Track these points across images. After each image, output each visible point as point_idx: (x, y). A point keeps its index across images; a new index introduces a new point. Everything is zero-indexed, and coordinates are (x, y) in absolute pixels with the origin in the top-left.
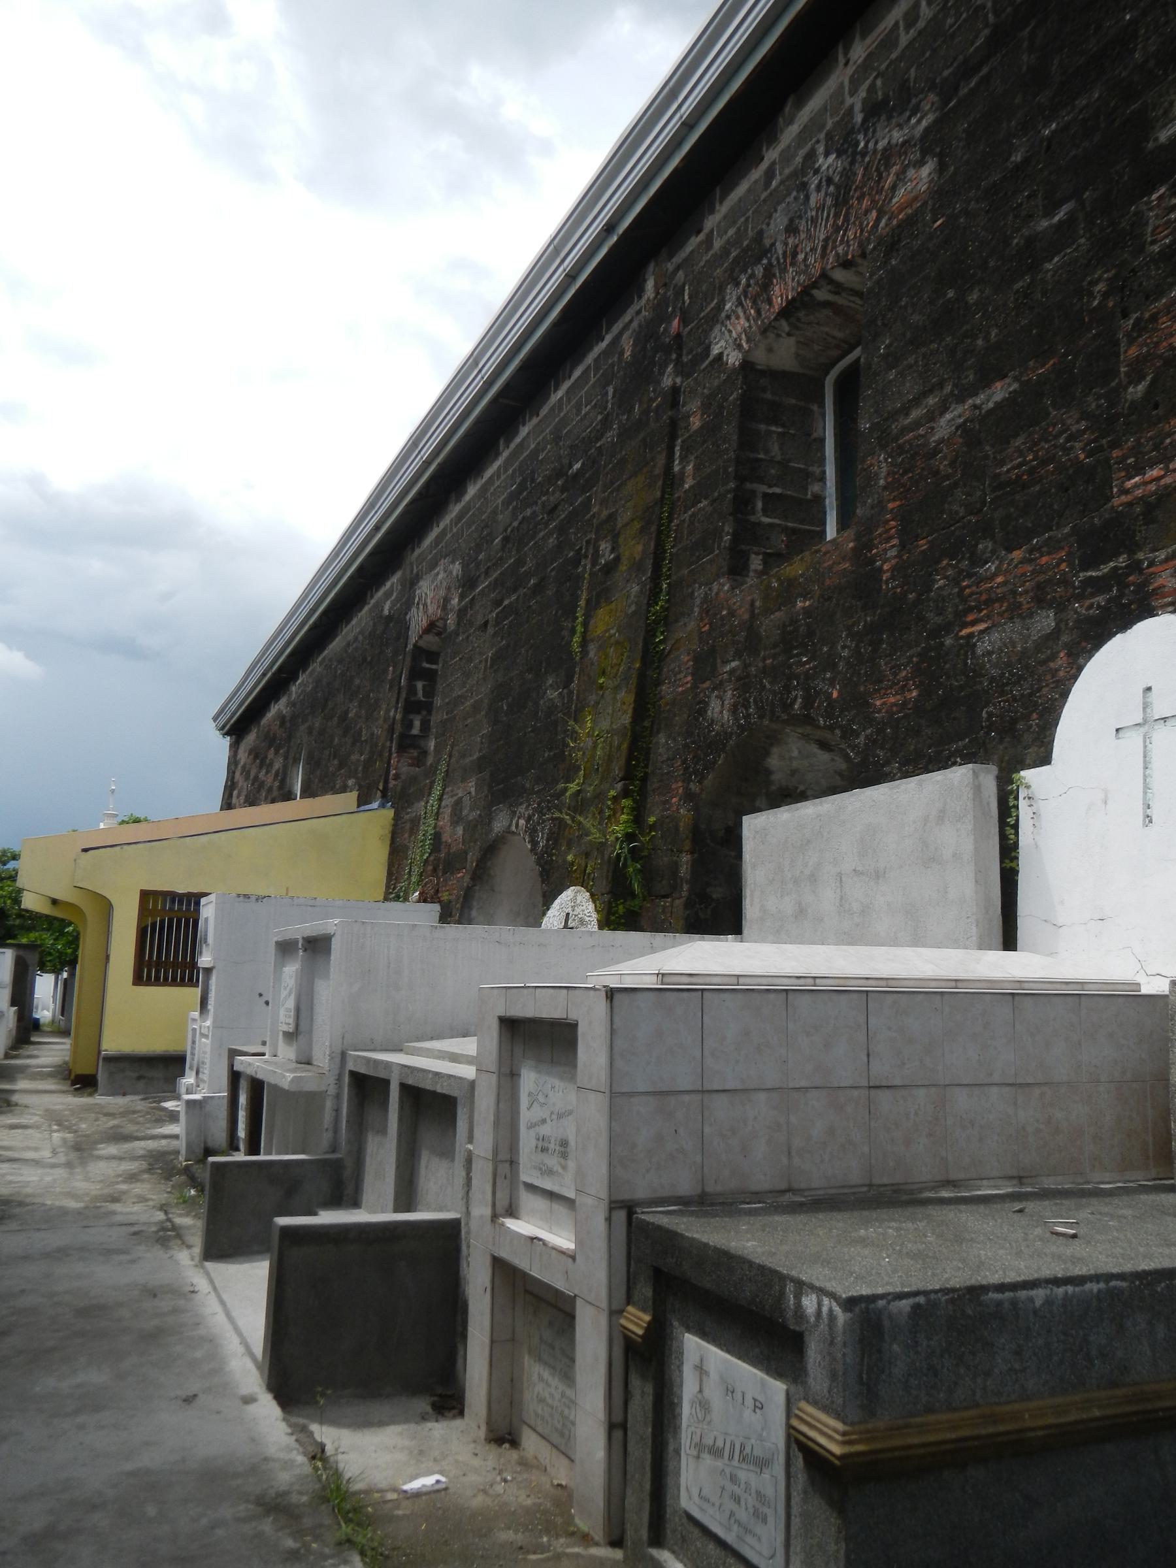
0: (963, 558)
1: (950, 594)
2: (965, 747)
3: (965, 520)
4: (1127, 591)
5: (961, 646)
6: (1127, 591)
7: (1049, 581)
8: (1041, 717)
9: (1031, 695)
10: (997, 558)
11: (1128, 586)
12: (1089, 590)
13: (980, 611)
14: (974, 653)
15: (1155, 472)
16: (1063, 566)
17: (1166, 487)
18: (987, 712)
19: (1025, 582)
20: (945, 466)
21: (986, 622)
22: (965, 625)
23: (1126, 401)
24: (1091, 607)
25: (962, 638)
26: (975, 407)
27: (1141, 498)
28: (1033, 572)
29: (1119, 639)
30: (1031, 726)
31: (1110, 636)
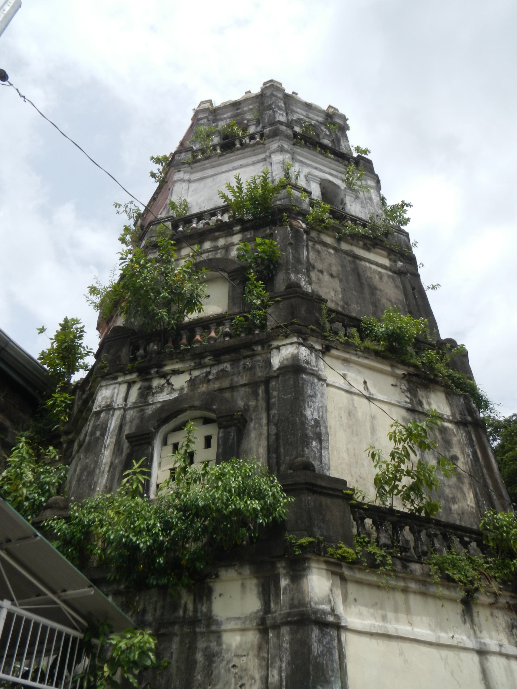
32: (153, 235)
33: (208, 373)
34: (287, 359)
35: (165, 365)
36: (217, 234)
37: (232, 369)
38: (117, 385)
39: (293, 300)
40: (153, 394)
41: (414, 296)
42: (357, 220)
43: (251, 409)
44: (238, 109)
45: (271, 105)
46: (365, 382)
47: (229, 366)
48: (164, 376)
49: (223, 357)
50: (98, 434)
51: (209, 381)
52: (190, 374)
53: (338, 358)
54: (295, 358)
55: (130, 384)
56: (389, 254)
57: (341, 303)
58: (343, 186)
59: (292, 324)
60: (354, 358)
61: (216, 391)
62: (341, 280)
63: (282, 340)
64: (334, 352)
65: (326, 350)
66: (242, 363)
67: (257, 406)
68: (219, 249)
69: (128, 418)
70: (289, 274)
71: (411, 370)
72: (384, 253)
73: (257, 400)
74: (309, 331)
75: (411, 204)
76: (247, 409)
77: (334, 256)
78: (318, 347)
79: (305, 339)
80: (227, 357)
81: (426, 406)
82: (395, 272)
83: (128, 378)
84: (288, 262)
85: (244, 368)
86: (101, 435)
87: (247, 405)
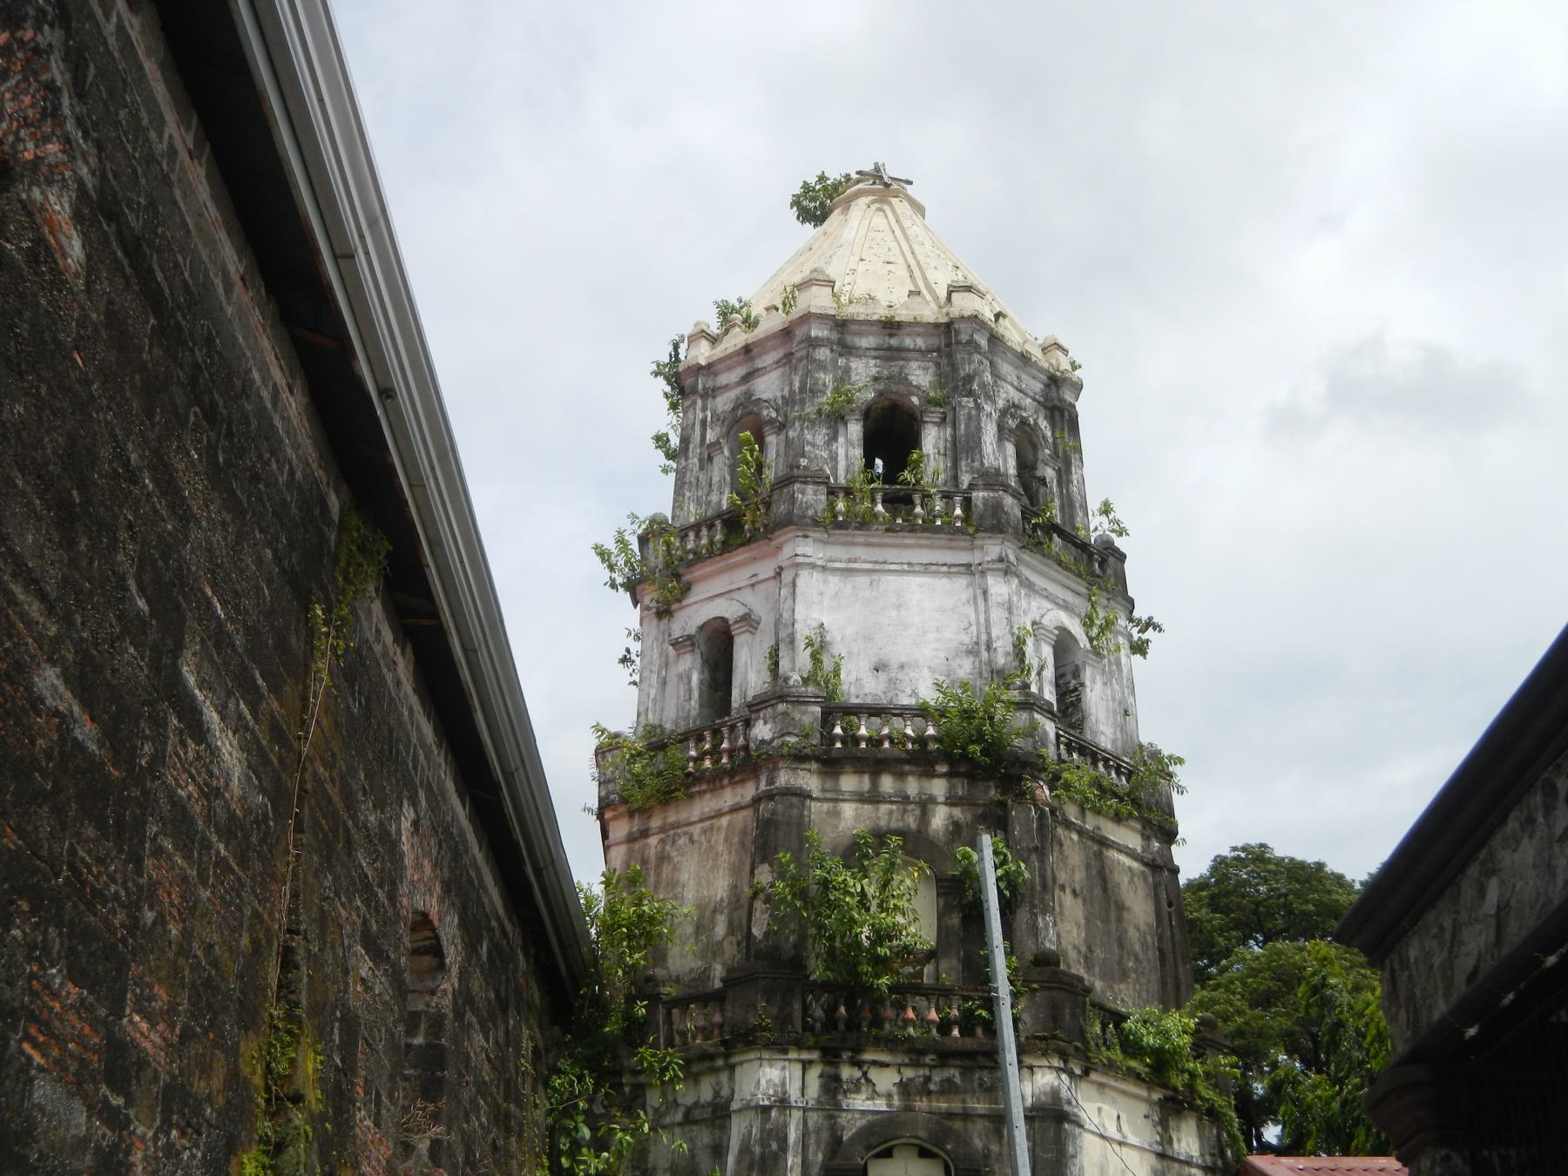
32: (791, 730)
33: (928, 1079)
34: (1045, 1093)
35: (864, 1051)
36: (907, 768)
37: (963, 1081)
38: (787, 1063)
39: (1055, 994)
40: (845, 1092)
41: (1171, 921)
42: (1109, 759)
43: (994, 1157)
44: (891, 335)
45: (969, 379)
46: (1119, 1117)
47: (957, 1075)
48: (858, 1064)
49: (952, 1062)
50: (774, 1146)
51: (929, 1093)
52: (899, 1072)
53: (1093, 1082)
54: (1055, 1093)
55: (806, 1065)
56: (1144, 827)
57: (1083, 949)
58: (1084, 642)
59: (1054, 1037)
60: (1112, 1083)
61: (940, 1114)
62: (1084, 901)
63: (1037, 1057)
64: (1094, 1076)
65: (1086, 1072)
66: (977, 1076)
67: (1000, 1154)
68: (911, 803)
69: (811, 1124)
70: (1036, 915)
71: (1170, 1093)
72: (1139, 826)
73: (1001, 1144)
74: (1072, 1051)
75: (1163, 627)
76: (987, 1156)
77: (1077, 848)
78: (1078, 1071)
79: (1065, 1062)
80: (959, 1063)
81: (1176, 1145)
82: (1146, 864)
83: (805, 1056)
84: (1033, 889)
85: (981, 1085)
86: (779, 1147)
87: (985, 1147)
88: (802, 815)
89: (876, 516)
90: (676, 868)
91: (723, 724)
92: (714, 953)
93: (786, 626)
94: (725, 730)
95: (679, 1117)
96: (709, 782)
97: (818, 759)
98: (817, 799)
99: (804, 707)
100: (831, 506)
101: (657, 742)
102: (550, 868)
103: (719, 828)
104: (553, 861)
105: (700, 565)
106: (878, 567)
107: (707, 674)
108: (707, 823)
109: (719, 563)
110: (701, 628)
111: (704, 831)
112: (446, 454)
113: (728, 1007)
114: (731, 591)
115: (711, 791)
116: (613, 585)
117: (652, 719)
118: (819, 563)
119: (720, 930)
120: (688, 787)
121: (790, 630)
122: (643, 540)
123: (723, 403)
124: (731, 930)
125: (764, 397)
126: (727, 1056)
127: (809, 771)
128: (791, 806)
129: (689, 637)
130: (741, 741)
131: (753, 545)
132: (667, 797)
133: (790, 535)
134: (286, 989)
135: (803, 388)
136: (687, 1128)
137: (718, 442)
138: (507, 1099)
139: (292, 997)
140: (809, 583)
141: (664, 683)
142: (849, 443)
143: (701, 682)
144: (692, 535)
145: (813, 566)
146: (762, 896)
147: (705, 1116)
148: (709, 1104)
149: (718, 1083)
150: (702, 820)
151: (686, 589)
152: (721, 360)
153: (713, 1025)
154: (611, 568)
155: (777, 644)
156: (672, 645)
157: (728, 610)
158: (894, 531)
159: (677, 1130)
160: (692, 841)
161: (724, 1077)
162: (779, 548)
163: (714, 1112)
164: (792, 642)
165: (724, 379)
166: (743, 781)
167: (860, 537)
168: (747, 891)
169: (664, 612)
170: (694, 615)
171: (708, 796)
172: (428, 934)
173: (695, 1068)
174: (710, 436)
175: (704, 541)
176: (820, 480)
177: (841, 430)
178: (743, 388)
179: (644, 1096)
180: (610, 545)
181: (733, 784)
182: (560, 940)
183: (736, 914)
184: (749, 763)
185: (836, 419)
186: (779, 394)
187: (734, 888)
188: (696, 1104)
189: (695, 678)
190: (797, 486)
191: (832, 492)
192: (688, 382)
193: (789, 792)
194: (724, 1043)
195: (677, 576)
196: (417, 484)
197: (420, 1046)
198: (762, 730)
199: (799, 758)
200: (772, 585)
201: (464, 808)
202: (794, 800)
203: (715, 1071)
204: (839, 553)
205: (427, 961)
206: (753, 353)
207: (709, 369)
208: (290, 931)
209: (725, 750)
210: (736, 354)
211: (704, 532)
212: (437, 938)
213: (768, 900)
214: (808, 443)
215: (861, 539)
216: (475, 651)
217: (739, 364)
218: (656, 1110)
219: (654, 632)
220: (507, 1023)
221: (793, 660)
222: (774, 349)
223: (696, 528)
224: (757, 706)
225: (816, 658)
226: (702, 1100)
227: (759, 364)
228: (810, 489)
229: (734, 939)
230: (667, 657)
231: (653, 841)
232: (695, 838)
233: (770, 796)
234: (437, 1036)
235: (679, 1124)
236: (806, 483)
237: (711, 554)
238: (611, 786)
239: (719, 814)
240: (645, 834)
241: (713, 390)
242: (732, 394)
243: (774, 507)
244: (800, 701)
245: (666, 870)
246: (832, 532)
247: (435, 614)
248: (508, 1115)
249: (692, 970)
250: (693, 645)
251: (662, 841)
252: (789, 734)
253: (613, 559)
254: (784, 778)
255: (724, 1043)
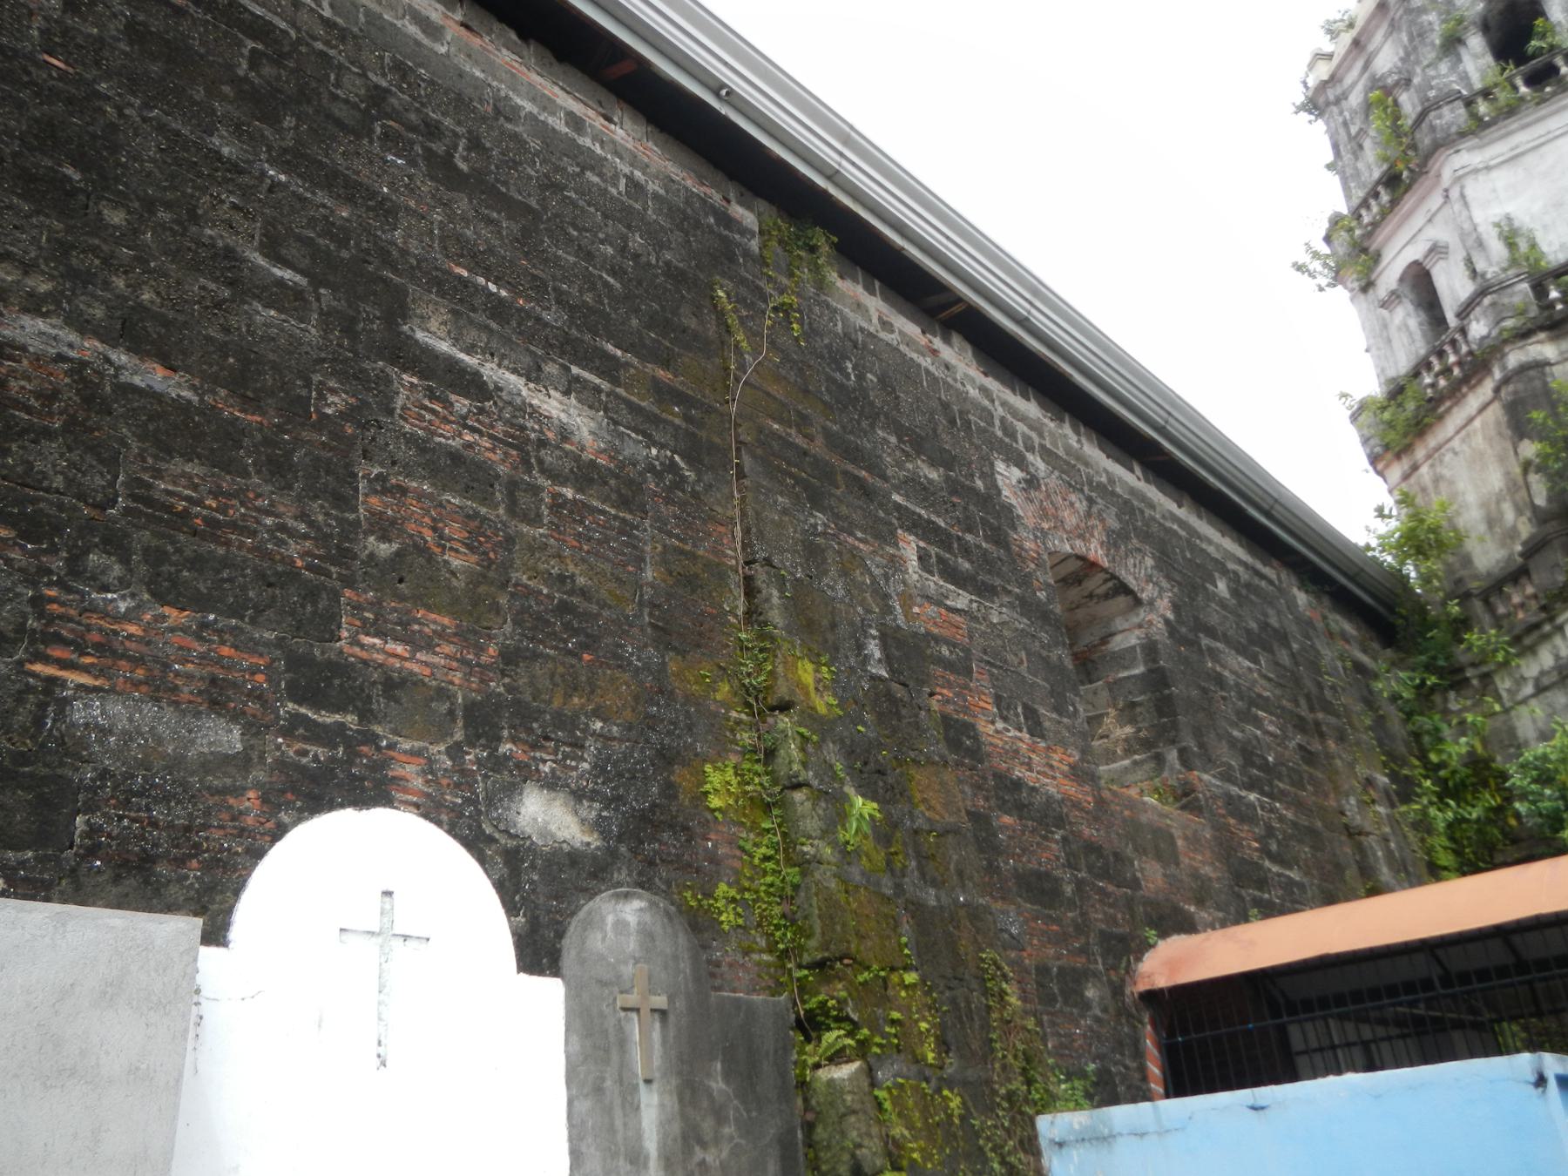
0: (53, 550)
1: (9, 590)
2: (22, 864)
3: (66, 500)
4: (358, 761)
5: (29, 689)
6: (358, 761)
7: (234, 685)
8: (207, 867)
9: (188, 829)
10: (133, 596)
11: (360, 755)
12: (301, 731)
13: (83, 654)
14: (61, 714)
15: (399, 649)
16: (260, 678)
17: (412, 673)
18: (88, 822)
19: (188, 661)
20: (23, 388)
21: (96, 678)
22: (47, 660)
23: (365, 547)
24: (305, 753)
25: (34, 675)
26: (108, 360)
27: (381, 665)
28: (202, 657)
29: (349, 813)
30: (186, 877)
31: (331, 806)
32: (1505, 315)
88: (1545, 384)
89: (1522, 99)
90: (1451, 483)
91: (1443, 343)
92: (1512, 538)
93: (1469, 234)
94: (1447, 348)
95: (1529, 689)
96: (1450, 398)
97: (1542, 328)
98: (1557, 363)
99: (1509, 290)
100: (1474, 116)
101: (1397, 391)
102: (1277, 507)
103: (1475, 431)
104: (1276, 501)
105: (1379, 230)
106: (1542, 140)
107: (1423, 316)
108: (1463, 433)
109: (1394, 220)
110: (1402, 280)
111: (1463, 441)
112: (849, 136)
113: (1535, 577)
114: (1415, 236)
115: (1456, 404)
116: (1321, 289)
117: (1392, 373)
118: (1481, 166)
119: (1509, 515)
120: (1435, 409)
121: (1474, 236)
122: (1328, 239)
123: (1355, 99)
124: (1519, 511)
125: (1385, 70)
126: (1551, 619)
127: (1538, 342)
128: (1531, 379)
129: (1393, 293)
130: (1464, 349)
131: (1415, 187)
132: (1420, 427)
133: (1442, 158)
134: (753, 615)
135: (1411, 39)
136: (1541, 697)
137: (1361, 129)
138: (1312, 709)
139: (761, 618)
140: (1473, 189)
141: (1389, 341)
142: (1475, 56)
143: (1421, 324)
144: (1363, 212)
145: (1476, 171)
146: (1532, 468)
147: (1554, 679)
148: (1554, 668)
149: (1555, 647)
150: (1458, 432)
151: (1377, 258)
152: (1339, 66)
153: (1528, 598)
154: (1312, 275)
155: (1468, 255)
156: (1382, 306)
157: (1415, 253)
158: (1547, 100)
159: (1533, 702)
160: (1456, 453)
161: (1558, 640)
162: (1439, 176)
163: (1560, 673)
164: (1480, 244)
165: (1348, 80)
166: (1480, 382)
167: (1513, 123)
168: (1518, 470)
169: (1367, 287)
170: (1390, 274)
171: (1455, 410)
172: (1103, 576)
173: (1527, 641)
174: (1354, 130)
175: (1375, 209)
176: (1451, 97)
177: (1462, 51)
178: (1366, 75)
179: (1493, 683)
180: (1304, 258)
181: (1472, 388)
182: (1345, 574)
183: (1517, 497)
184: (1476, 366)
185: (1452, 43)
186: (1396, 59)
187: (1507, 474)
188: (1543, 673)
189: (1413, 323)
190: (1432, 114)
191: (1469, 103)
192: (1321, 100)
193: (1523, 368)
194: (1544, 608)
195: (1365, 250)
196: (833, 175)
197: (1143, 674)
198: (1479, 328)
199: (1523, 335)
200: (1446, 211)
201: (1132, 471)
202: (1532, 373)
203: (1546, 637)
204: (1498, 150)
205: (1122, 601)
206: (1363, 39)
207: (1333, 79)
208: (747, 563)
209: (1454, 364)
210: (1349, 52)
211: (1373, 202)
212: (1113, 577)
213: (1539, 470)
214: (1434, 78)
215: (1515, 126)
216: (1027, 319)
217: (1355, 60)
218: (1509, 691)
219: (1364, 305)
220: (1289, 647)
221: (1488, 259)
222: (1377, 27)
223: (1365, 204)
224: (1465, 312)
225: (1511, 245)
226: (1546, 668)
227: (1371, 48)
228: (1446, 110)
229: (1524, 519)
230: (1384, 319)
231: (1424, 470)
232: (1457, 450)
233: (1506, 381)
234: (1155, 661)
235: (1534, 696)
236: (1439, 107)
237: (1385, 214)
238: (1372, 442)
239: (1471, 420)
240: (1415, 468)
241: (1343, 93)
242: (1360, 87)
243: (1420, 146)
244: (1503, 287)
245: (1443, 486)
246: (1483, 134)
247: (959, 300)
248: (1317, 724)
249: (1498, 562)
250: (1398, 297)
251: (1432, 466)
252: (1503, 319)
253: (1311, 268)
254: (1514, 358)
255: (1544, 608)
